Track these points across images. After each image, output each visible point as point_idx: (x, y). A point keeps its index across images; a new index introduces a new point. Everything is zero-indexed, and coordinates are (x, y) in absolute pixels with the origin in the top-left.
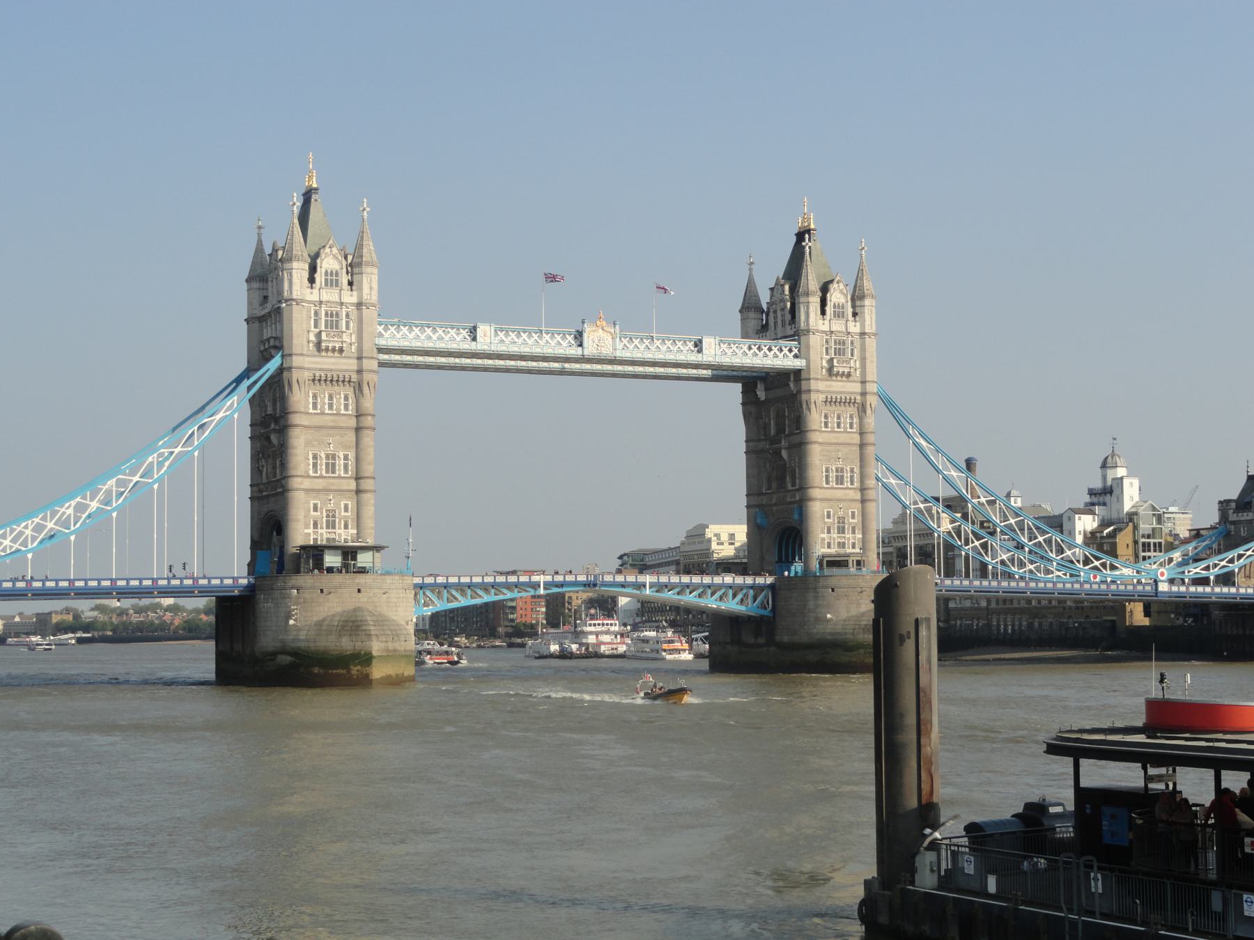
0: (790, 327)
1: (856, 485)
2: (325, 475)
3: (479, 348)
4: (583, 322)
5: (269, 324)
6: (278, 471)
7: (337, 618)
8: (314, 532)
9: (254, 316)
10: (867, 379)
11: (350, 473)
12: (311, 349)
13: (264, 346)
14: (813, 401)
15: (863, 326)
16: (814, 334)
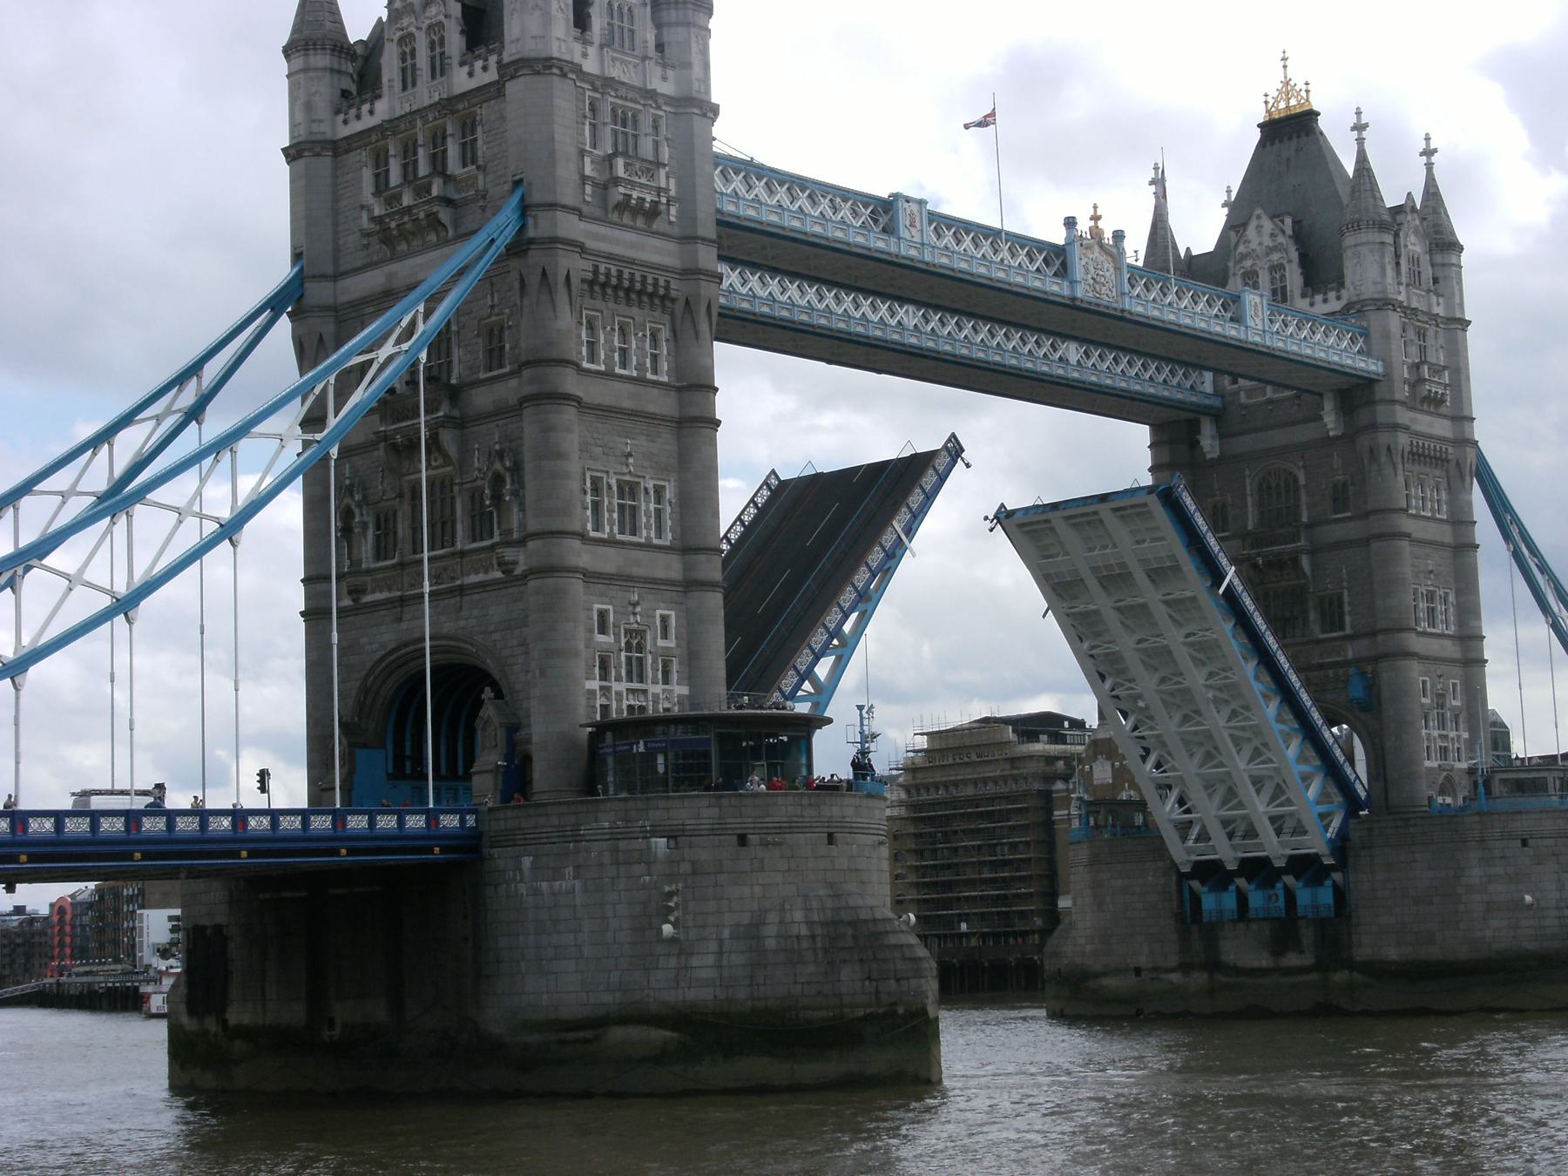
0: (1307, 300)
1: (1452, 630)
2: (619, 537)
3: (903, 253)
4: (1070, 223)
5: (392, 152)
6: (459, 527)
7: (798, 915)
8: (602, 688)
9: (319, 137)
10: (1466, 413)
11: (670, 535)
12: (588, 199)
13: (397, 197)
14: (1400, 448)
15: (1449, 305)
16: (1395, 310)
